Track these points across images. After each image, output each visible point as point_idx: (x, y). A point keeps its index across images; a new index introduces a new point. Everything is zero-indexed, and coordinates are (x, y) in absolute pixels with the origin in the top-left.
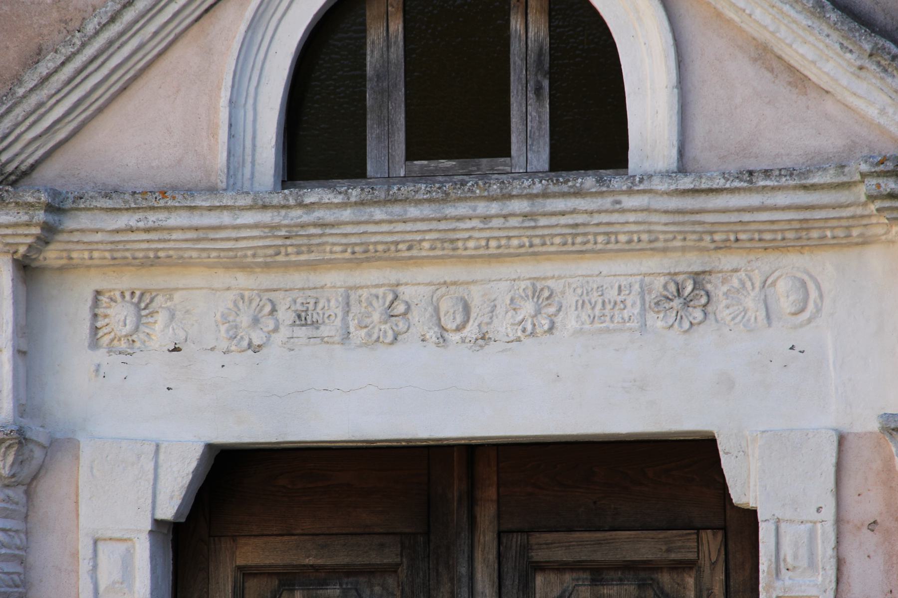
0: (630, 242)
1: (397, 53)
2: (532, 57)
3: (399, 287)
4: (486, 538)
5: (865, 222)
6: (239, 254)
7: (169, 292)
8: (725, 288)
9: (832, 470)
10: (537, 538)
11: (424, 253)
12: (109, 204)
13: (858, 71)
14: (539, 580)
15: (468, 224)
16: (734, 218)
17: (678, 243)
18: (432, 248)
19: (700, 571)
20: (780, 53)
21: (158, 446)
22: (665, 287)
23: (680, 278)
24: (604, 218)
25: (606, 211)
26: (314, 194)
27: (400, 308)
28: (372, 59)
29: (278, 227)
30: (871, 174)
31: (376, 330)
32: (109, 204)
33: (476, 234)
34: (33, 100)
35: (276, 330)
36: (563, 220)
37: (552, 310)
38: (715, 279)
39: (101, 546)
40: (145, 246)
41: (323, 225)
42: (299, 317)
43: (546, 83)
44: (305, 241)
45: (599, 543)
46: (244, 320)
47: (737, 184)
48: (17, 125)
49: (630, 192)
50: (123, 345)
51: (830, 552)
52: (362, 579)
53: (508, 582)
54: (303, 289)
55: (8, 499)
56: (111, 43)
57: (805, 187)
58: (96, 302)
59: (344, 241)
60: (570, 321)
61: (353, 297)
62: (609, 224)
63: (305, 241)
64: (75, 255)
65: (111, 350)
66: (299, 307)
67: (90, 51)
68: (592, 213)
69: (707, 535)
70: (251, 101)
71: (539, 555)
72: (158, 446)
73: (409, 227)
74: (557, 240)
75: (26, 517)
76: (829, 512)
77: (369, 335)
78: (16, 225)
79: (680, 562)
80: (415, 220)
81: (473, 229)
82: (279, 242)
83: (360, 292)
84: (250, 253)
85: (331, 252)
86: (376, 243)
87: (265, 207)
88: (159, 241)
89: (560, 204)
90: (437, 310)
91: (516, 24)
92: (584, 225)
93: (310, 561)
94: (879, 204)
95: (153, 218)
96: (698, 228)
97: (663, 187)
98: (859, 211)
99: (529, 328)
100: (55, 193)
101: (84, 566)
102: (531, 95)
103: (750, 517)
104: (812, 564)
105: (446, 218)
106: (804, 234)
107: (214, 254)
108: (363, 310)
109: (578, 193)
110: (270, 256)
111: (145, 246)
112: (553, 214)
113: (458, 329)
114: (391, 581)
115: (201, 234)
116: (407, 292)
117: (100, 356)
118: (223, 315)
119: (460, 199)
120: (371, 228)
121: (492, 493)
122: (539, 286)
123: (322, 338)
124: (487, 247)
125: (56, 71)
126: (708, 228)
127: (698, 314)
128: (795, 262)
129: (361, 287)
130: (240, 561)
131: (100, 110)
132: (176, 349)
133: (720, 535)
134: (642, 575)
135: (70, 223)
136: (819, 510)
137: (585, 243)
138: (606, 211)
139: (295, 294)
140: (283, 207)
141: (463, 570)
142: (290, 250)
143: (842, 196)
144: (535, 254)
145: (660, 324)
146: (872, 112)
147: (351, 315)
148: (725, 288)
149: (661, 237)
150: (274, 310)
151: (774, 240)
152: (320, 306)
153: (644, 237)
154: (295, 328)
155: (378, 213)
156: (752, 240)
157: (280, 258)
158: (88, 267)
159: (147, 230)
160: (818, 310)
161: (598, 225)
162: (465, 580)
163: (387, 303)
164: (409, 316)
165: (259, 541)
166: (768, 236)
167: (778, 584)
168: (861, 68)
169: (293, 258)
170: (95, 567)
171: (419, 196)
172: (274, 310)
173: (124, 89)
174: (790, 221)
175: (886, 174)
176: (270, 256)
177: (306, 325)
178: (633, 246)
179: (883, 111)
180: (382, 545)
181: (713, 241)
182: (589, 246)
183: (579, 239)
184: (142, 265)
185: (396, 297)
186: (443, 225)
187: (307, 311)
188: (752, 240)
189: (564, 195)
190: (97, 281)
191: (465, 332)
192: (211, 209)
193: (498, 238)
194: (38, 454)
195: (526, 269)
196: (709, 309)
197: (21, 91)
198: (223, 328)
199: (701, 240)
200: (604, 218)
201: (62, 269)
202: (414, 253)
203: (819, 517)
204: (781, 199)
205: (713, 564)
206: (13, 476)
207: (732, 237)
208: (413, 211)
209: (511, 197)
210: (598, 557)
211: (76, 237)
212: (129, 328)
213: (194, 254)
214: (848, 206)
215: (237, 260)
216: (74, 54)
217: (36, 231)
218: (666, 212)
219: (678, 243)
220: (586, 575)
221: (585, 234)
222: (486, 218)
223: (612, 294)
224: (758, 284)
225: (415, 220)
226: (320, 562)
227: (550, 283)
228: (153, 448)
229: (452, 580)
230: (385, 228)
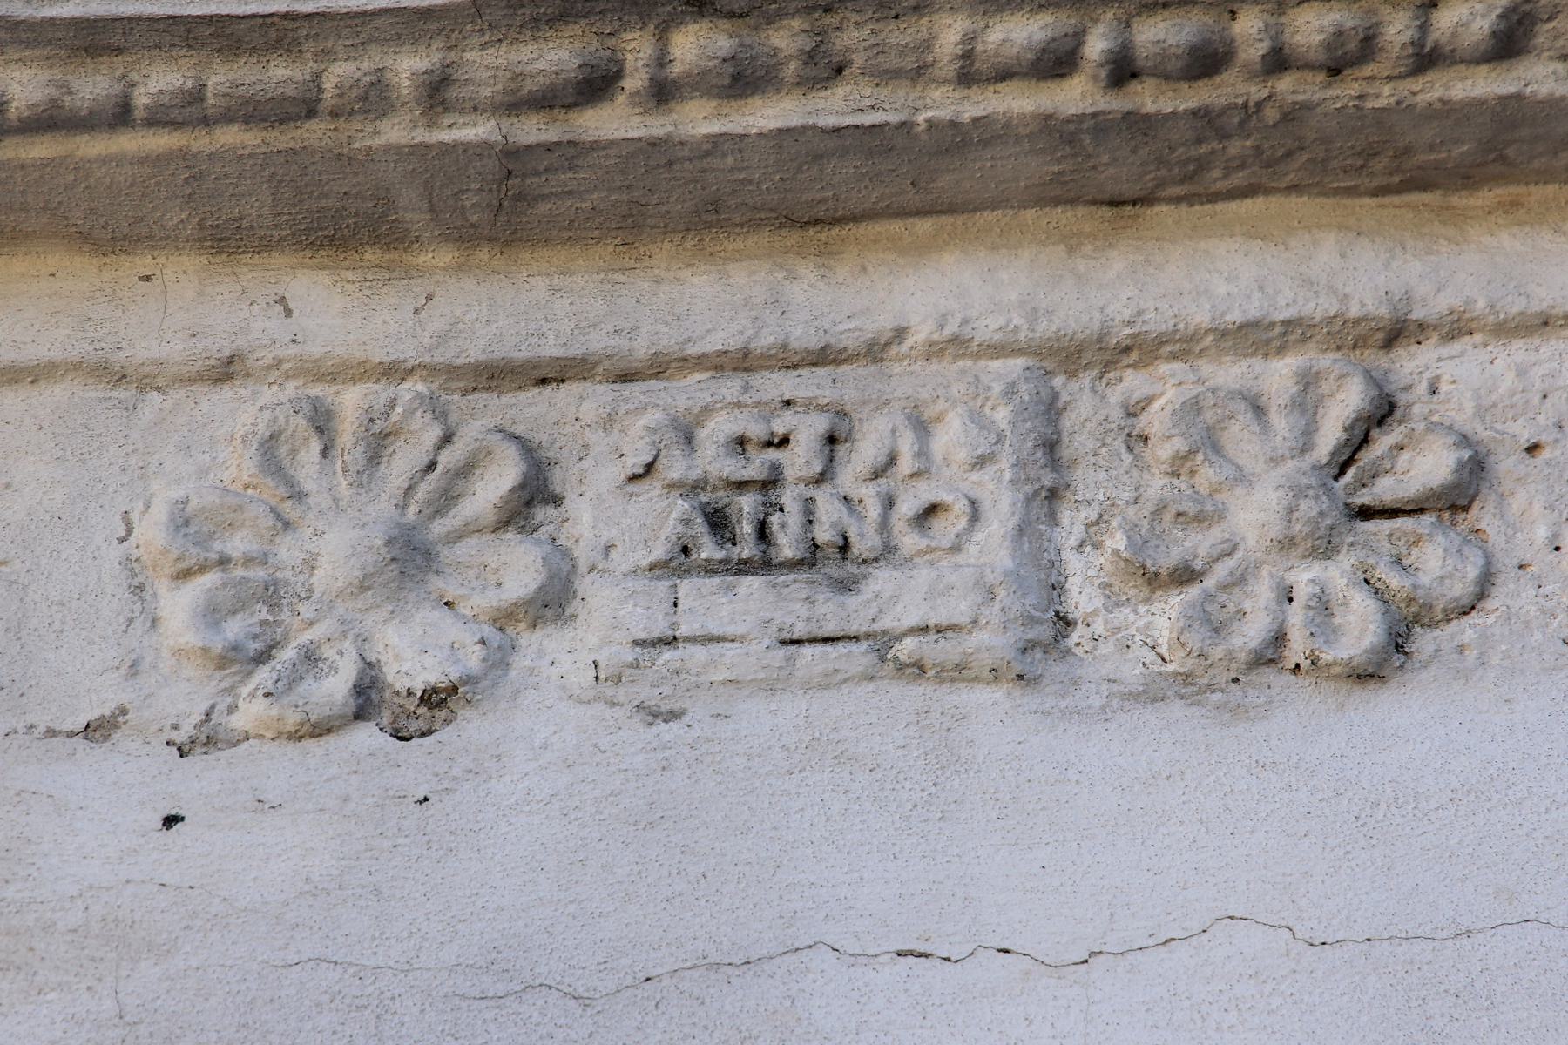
3: (1399, 352)
6: (340, 73)
31: (1262, 592)
42: (718, 521)
54: (743, 362)
66: (713, 460)
83: (1133, 383)
85: (969, 74)
108: (1156, 485)
110: (546, 101)
118: (182, 520)
123: (882, 642)
139: (688, 391)
147: (1072, 522)
152: (864, 452)
154: (686, 586)
163: (1330, 436)
164: (1484, 516)
176: (546, 101)
177: (765, 565)
187: (770, 483)
215: (315, 132)
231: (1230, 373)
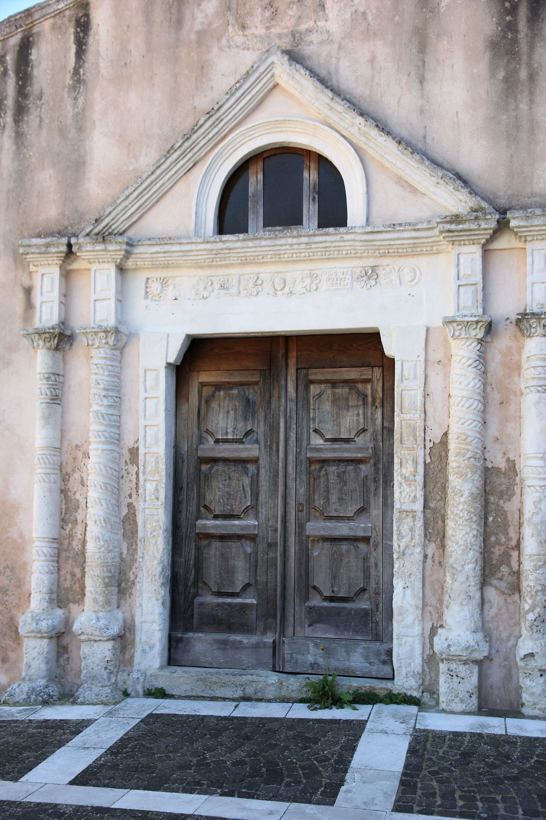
0: (347, 254)
1: (260, 186)
2: (312, 186)
4: (292, 371)
5: (439, 243)
7: (174, 278)
8: (384, 272)
9: (424, 341)
10: (311, 371)
11: (268, 260)
12: (149, 242)
13: (435, 184)
14: (312, 387)
15: (285, 248)
16: (387, 243)
17: (366, 254)
18: (271, 258)
19: (373, 383)
20: (406, 179)
21: (168, 335)
22: (361, 272)
23: (366, 269)
24: (337, 244)
25: (338, 241)
26: (225, 237)
27: (259, 282)
28: (251, 189)
29: (211, 250)
30: (441, 223)
32: (149, 242)
33: (288, 252)
34: (123, 205)
35: (213, 291)
36: (321, 245)
37: (317, 282)
38: (380, 268)
39: (147, 372)
40: (164, 259)
41: (230, 249)
43: (317, 197)
44: (223, 256)
45: (335, 372)
46: (201, 288)
47: (388, 229)
48: (118, 214)
49: (347, 233)
50: (157, 298)
51: (422, 372)
52: (246, 387)
53: (300, 388)
55: (113, 354)
56: (152, 182)
57: (415, 230)
58: (147, 282)
59: (238, 255)
60: (324, 286)
61: (242, 278)
62: (339, 246)
63: (223, 256)
64: (138, 263)
65: (152, 300)
66: (221, 282)
67: (144, 186)
68: (332, 242)
69: (376, 369)
70: (204, 204)
71: (312, 377)
72: (168, 335)
73: (262, 249)
74: (319, 254)
75: (121, 362)
76: (422, 358)
77: (248, 293)
78: (115, 251)
79: (366, 379)
80: (264, 246)
81: (286, 249)
82: (213, 256)
84: (202, 261)
86: (250, 256)
87: (208, 242)
88: (169, 257)
89: (320, 239)
90: (273, 282)
91: (306, 174)
92: (329, 247)
93: (226, 380)
94: (444, 235)
95: (166, 248)
96: (373, 248)
97: (359, 231)
98: (436, 239)
99: (308, 289)
100: (130, 239)
101: (141, 380)
102: (311, 201)
103: (392, 361)
104: (415, 377)
105: (276, 245)
106: (414, 249)
107: (189, 262)
109: (327, 234)
111: (164, 259)
112: (317, 243)
113: (281, 290)
114: (256, 388)
115: (184, 254)
116: (262, 276)
117: (148, 302)
119: (281, 238)
120: (248, 250)
121: (294, 354)
122: (312, 273)
124: (292, 257)
125: (132, 193)
126: (377, 247)
127: (373, 282)
128: (411, 261)
129: (245, 274)
130: (201, 380)
131: (149, 210)
132: (176, 299)
133: (381, 369)
134: (351, 384)
135: (136, 250)
136: (418, 356)
137: (330, 255)
138: (338, 241)
140: (215, 242)
141: (283, 383)
142: (218, 259)
143: (430, 233)
144: (311, 260)
145: (358, 286)
146: (442, 201)
148: (384, 272)
149: (359, 252)
150: (212, 284)
151: (403, 252)
153: (353, 252)
155: (250, 244)
156: (394, 252)
157: (214, 263)
158: (144, 269)
159: (164, 253)
160: (420, 280)
161: (335, 247)
162: (284, 387)
165: (208, 373)
166: (400, 251)
167: (402, 385)
168: (438, 183)
169: (219, 263)
170: (145, 380)
171: (266, 237)
172: (212, 284)
173: (158, 201)
174: (409, 244)
175: (447, 222)
178: (349, 255)
179: (446, 201)
180: (253, 374)
181: (379, 253)
182: (331, 256)
183: (327, 253)
184: (163, 268)
185: (258, 278)
186: (275, 248)
188: (394, 252)
189: (321, 235)
190: (147, 274)
191: (284, 291)
192: (188, 243)
193: (296, 253)
194: (124, 338)
195: (307, 266)
196: (378, 280)
197: (119, 201)
198: (193, 291)
199: (375, 253)
200: (337, 244)
201: (134, 270)
202: (265, 260)
203: (418, 359)
204: (406, 235)
205: (378, 380)
206: (115, 345)
207: (387, 251)
208: (264, 243)
209: (301, 236)
210: (334, 378)
211: (138, 256)
212: (159, 291)
213: (182, 262)
214: (432, 237)
216: (138, 187)
217: (123, 253)
218: (361, 241)
219: (366, 254)
220: (330, 385)
221: (330, 251)
222: (291, 245)
223: (340, 275)
224: (397, 270)
225: (264, 246)
226: (230, 380)
227: (317, 272)
228: (166, 336)
229: (279, 387)
230: (253, 250)
231: (250, 276)
